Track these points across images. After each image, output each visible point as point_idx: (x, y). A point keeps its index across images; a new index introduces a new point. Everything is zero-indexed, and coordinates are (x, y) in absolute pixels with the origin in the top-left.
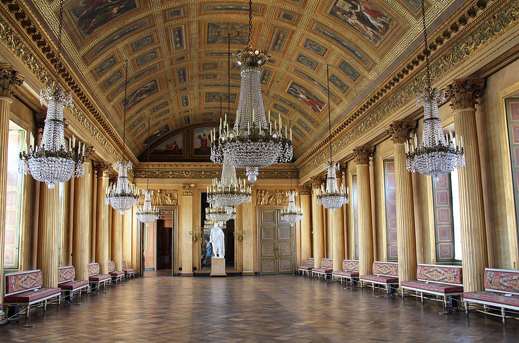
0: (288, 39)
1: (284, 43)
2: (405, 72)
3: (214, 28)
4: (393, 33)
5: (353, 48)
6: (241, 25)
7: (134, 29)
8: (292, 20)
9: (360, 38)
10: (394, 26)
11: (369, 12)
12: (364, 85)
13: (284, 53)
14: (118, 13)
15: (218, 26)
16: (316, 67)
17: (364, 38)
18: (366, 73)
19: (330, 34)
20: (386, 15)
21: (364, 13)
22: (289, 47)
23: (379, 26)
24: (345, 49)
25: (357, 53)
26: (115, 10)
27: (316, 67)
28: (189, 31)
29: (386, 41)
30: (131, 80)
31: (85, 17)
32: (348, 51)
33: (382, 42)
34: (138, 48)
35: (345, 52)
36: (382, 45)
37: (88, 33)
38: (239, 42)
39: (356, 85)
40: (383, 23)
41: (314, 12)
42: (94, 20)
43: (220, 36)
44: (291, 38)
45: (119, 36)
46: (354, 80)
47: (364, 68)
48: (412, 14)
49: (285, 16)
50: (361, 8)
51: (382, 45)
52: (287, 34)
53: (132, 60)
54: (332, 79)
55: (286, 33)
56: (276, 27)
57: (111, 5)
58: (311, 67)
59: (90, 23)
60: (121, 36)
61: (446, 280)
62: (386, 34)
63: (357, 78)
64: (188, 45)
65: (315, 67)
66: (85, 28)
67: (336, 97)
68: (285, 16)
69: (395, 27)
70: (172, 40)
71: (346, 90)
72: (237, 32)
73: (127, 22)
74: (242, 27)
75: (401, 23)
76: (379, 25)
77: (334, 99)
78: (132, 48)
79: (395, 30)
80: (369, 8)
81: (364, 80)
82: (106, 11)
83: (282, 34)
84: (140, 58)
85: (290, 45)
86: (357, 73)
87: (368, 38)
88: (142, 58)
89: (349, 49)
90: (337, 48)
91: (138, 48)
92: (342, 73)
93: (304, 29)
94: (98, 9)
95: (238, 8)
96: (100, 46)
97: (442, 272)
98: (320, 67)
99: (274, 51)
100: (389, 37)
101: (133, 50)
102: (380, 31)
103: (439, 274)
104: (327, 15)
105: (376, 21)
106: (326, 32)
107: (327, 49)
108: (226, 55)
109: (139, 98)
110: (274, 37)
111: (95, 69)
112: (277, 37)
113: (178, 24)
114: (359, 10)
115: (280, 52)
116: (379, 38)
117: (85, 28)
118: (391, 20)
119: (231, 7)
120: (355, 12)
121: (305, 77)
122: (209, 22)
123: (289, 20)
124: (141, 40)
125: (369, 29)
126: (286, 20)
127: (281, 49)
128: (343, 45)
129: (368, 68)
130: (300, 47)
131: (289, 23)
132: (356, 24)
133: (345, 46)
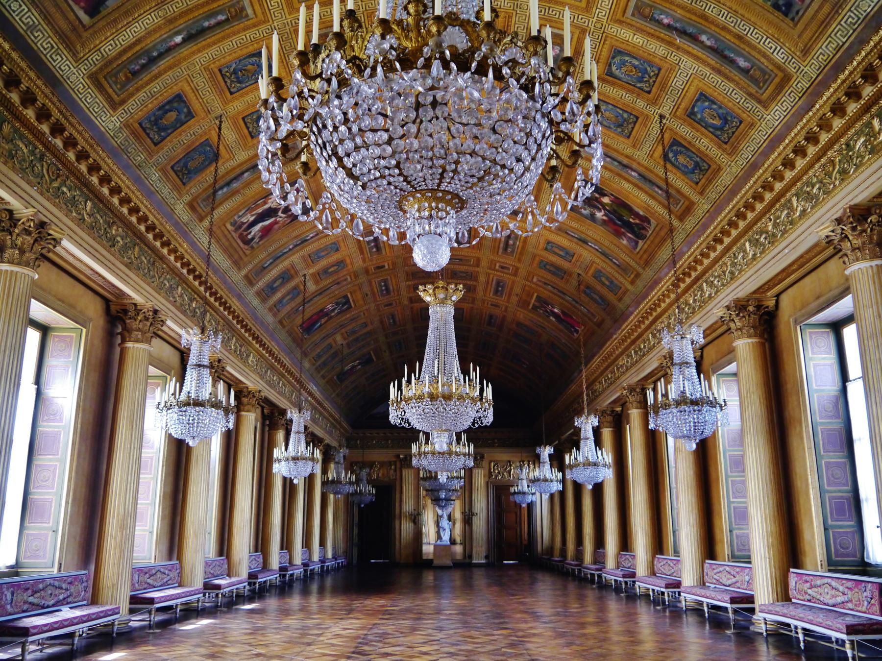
2: (185, 265)
4: (238, 249)
5: (235, 185)
9: (244, 202)
10: (246, 251)
11: (272, 225)
12: (166, 191)
14: (605, 195)
16: (226, 82)
17: (244, 208)
18: (187, 198)
20: (260, 243)
21: (272, 220)
23: (251, 232)
24: (238, 171)
25: (225, 190)
26: (606, 200)
27: (226, 82)
29: (231, 239)
30: (708, 43)
31: (633, 233)
32: (233, 175)
33: (230, 233)
34: (625, 115)
35: (234, 169)
36: (226, 232)
37: (649, 222)
39: (163, 170)
40: (253, 239)
42: (631, 220)
45: (630, 171)
46: (175, 168)
47: (196, 197)
48: (251, 270)
50: (281, 217)
51: (226, 232)
53: (654, 102)
54: (183, 105)
57: (605, 209)
58: (232, 69)
59: (636, 224)
60: (626, 166)
61: (169, 582)
62: (239, 241)
63: (178, 176)
65: (227, 80)
66: (644, 228)
67: (123, 86)
69: (244, 253)
71: (148, 135)
75: (246, 259)
76: (252, 234)
77: (116, 76)
78: (633, 128)
79: (241, 253)
80: (276, 227)
81: (175, 193)
82: (615, 211)
84: (639, 88)
86: (190, 178)
87: (240, 214)
88: (638, 85)
89: (236, 178)
90: (246, 157)
91: (625, 115)
92: (193, 143)
94: (619, 221)
96: (657, 193)
97: (167, 572)
98: (221, 93)
100: (235, 245)
101: (635, 123)
102: (245, 233)
103: (164, 576)
105: (259, 231)
107: (252, 137)
111: (697, 183)
114: (280, 214)
116: (236, 230)
117: (644, 228)
118: (252, 247)
120: (280, 209)
121: (209, 16)
124: (610, 128)
125: (252, 219)
128: (247, 171)
129: (195, 204)
132: (265, 203)
133: (243, 173)
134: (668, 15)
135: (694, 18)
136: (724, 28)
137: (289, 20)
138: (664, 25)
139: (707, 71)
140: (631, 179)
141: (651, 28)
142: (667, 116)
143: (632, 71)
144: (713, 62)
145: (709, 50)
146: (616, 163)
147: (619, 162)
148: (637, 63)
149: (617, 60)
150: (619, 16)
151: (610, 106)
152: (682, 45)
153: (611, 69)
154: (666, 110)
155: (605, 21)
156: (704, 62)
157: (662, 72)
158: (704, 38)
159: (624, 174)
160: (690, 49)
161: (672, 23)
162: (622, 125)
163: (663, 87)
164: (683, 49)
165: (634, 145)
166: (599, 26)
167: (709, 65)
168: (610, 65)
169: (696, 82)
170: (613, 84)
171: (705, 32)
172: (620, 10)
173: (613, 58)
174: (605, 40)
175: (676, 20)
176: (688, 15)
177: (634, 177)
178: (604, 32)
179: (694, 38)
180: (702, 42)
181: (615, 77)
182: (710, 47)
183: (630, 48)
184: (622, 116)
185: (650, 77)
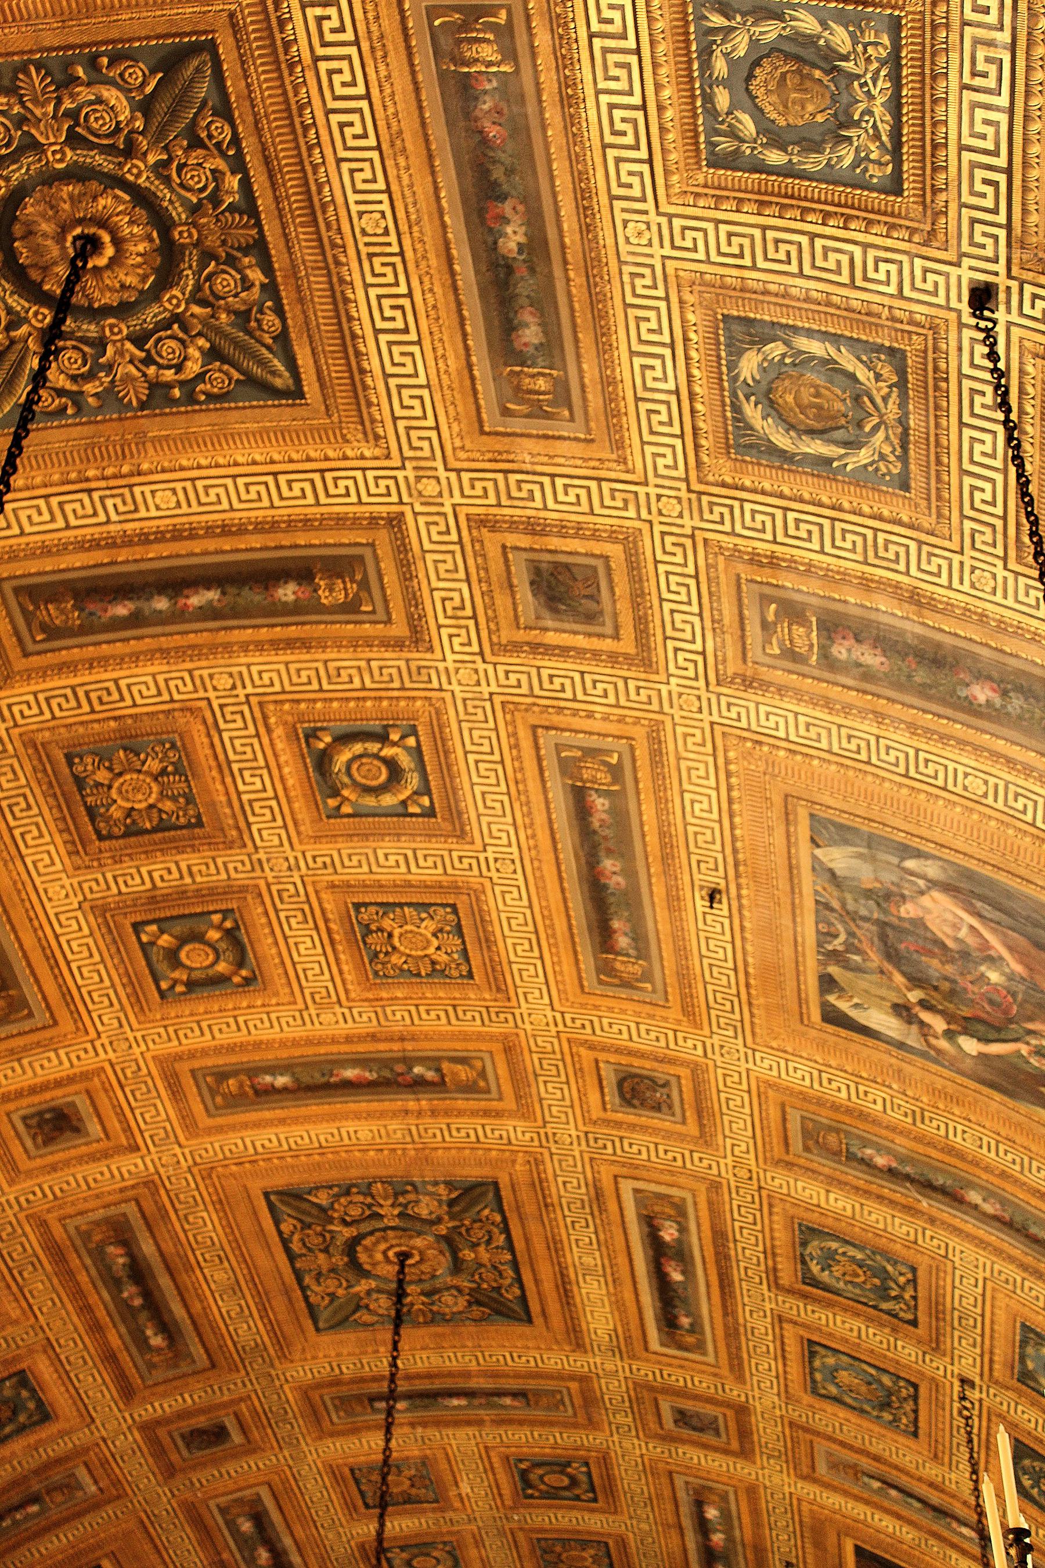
0: (115, 1341)
1: (111, 1306)
3: (495, 1295)
6: (367, 1318)
7: (884, 1482)
8: (183, 1436)
13: (56, 1252)
15: (479, 1303)
19: (16, 1523)
22: (69, 1307)
28: (619, 1305)
30: (988, 1208)
34: (886, 1380)
38: (322, 1199)
41: (142, 1522)
43: (448, 1240)
44: (110, 1358)
45: (954, 1525)
49: (219, 1434)
52: (143, 1367)
55: (151, 1366)
56: (213, 1366)
64: (612, 1206)
68: (219, 1434)
70: (708, 1286)
72: (363, 1273)
73: (908, 1534)
74: (358, 1308)
83: (159, 1350)
84: (888, 1313)
85: (75, 1319)
88: (885, 1306)
93: (104, 1440)
95: (426, 1401)
99: (107, 1221)
101: (915, 1398)
104: (99, 1553)
106: (34, 1508)
108: (350, 1073)
109: (993, 961)
110: (178, 1310)
112: (166, 1317)
113: (681, 1367)
115: (78, 1242)
119: (455, 1402)
122: (526, 1329)
123: (192, 1432)
124: (862, 1411)
126: (201, 1421)
127: (88, 1261)
130: (31, 1352)
131: (182, 1415)
134: (879, 1148)
135: (934, 1153)
136: (1003, 1175)
137: (12, 1197)
138: (880, 1170)
139: (1012, 1272)
140: (966, 1546)
141: (855, 1175)
142: (977, 1380)
143: (857, 1275)
144: (1016, 1253)
145: (997, 1224)
146: (917, 1505)
147: (919, 1500)
148: (859, 1256)
149: (814, 1247)
150: (778, 1151)
151: (845, 1358)
152: (934, 1212)
153: (809, 1270)
154: (968, 1364)
155: (753, 1162)
156: (998, 1252)
157: (921, 1274)
158: (974, 1197)
159: (946, 1533)
160: (957, 1222)
161: (894, 1165)
162: (889, 1405)
163: (938, 1311)
164: (943, 1223)
165: (936, 1456)
166: (743, 1174)
167: (1011, 1259)
168: (804, 1262)
169: (1002, 1301)
170: (830, 1305)
171: (971, 1185)
172: (775, 1140)
173: (804, 1244)
174: (771, 1206)
175: (903, 1160)
176: (921, 1148)
177: (970, 1539)
178: (760, 1188)
179: (954, 1197)
180: (976, 1207)
181: (826, 1288)
182: (995, 1218)
183: (830, 1222)
184: (880, 1382)
185: (902, 1288)
